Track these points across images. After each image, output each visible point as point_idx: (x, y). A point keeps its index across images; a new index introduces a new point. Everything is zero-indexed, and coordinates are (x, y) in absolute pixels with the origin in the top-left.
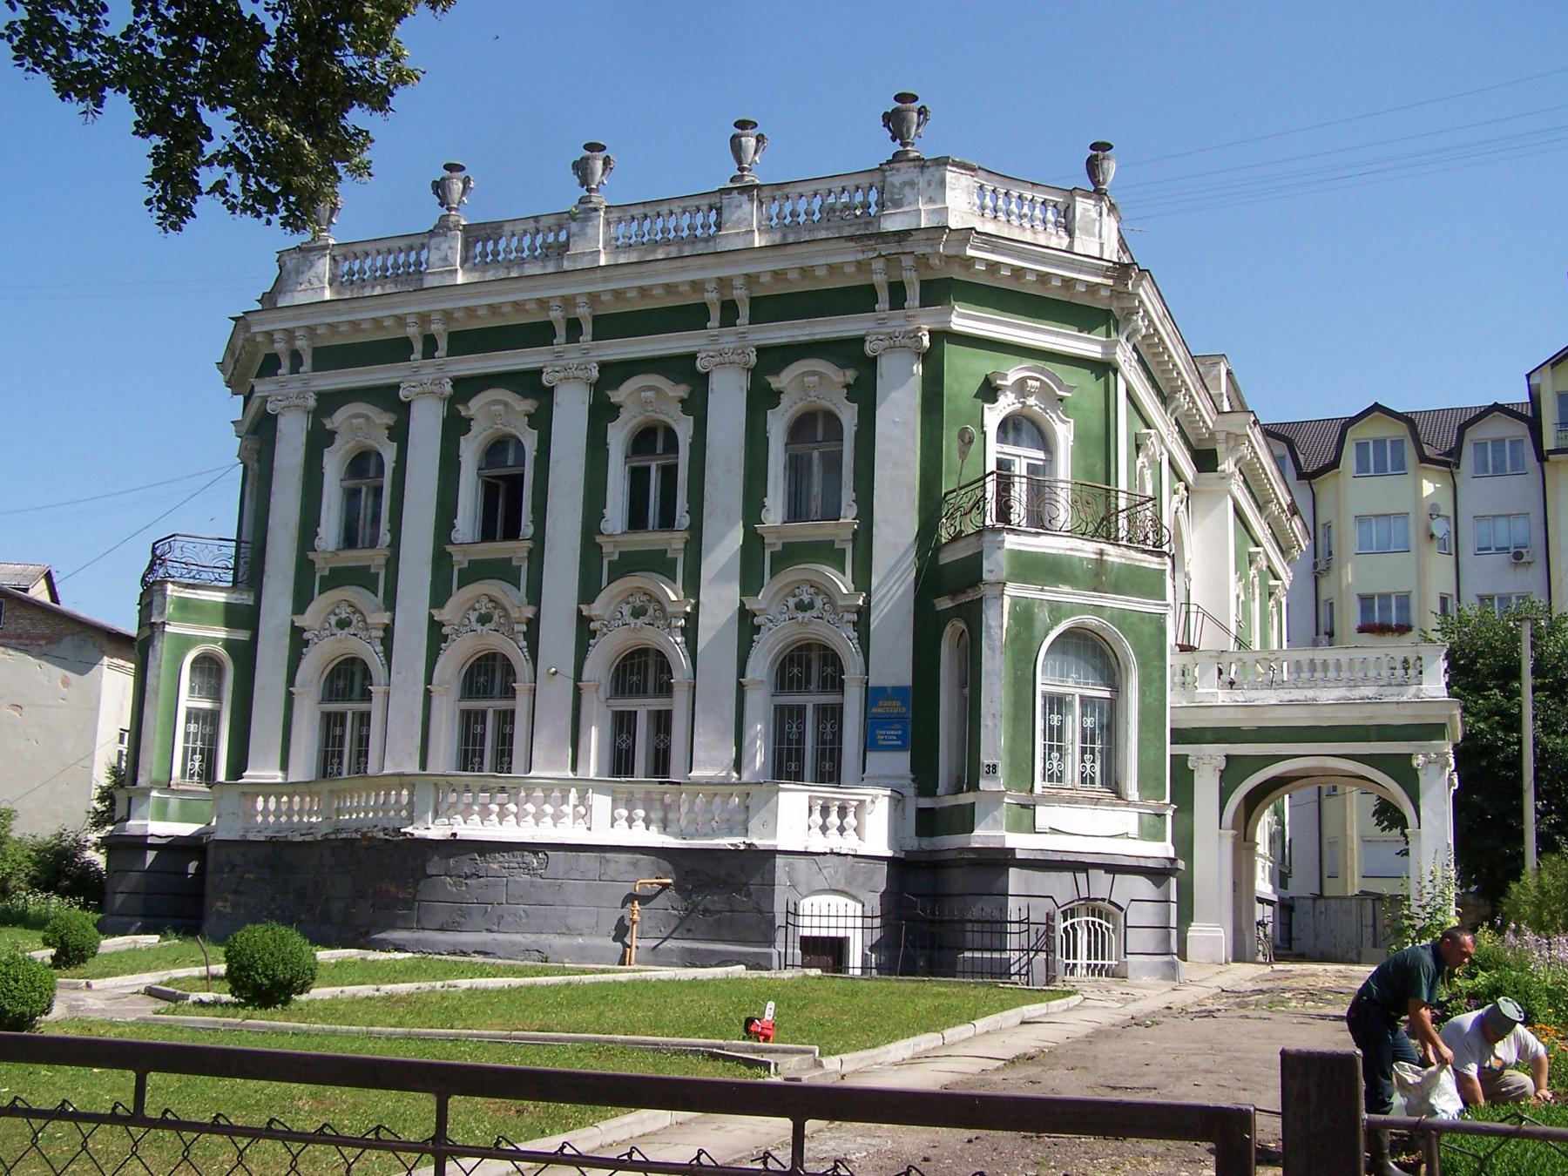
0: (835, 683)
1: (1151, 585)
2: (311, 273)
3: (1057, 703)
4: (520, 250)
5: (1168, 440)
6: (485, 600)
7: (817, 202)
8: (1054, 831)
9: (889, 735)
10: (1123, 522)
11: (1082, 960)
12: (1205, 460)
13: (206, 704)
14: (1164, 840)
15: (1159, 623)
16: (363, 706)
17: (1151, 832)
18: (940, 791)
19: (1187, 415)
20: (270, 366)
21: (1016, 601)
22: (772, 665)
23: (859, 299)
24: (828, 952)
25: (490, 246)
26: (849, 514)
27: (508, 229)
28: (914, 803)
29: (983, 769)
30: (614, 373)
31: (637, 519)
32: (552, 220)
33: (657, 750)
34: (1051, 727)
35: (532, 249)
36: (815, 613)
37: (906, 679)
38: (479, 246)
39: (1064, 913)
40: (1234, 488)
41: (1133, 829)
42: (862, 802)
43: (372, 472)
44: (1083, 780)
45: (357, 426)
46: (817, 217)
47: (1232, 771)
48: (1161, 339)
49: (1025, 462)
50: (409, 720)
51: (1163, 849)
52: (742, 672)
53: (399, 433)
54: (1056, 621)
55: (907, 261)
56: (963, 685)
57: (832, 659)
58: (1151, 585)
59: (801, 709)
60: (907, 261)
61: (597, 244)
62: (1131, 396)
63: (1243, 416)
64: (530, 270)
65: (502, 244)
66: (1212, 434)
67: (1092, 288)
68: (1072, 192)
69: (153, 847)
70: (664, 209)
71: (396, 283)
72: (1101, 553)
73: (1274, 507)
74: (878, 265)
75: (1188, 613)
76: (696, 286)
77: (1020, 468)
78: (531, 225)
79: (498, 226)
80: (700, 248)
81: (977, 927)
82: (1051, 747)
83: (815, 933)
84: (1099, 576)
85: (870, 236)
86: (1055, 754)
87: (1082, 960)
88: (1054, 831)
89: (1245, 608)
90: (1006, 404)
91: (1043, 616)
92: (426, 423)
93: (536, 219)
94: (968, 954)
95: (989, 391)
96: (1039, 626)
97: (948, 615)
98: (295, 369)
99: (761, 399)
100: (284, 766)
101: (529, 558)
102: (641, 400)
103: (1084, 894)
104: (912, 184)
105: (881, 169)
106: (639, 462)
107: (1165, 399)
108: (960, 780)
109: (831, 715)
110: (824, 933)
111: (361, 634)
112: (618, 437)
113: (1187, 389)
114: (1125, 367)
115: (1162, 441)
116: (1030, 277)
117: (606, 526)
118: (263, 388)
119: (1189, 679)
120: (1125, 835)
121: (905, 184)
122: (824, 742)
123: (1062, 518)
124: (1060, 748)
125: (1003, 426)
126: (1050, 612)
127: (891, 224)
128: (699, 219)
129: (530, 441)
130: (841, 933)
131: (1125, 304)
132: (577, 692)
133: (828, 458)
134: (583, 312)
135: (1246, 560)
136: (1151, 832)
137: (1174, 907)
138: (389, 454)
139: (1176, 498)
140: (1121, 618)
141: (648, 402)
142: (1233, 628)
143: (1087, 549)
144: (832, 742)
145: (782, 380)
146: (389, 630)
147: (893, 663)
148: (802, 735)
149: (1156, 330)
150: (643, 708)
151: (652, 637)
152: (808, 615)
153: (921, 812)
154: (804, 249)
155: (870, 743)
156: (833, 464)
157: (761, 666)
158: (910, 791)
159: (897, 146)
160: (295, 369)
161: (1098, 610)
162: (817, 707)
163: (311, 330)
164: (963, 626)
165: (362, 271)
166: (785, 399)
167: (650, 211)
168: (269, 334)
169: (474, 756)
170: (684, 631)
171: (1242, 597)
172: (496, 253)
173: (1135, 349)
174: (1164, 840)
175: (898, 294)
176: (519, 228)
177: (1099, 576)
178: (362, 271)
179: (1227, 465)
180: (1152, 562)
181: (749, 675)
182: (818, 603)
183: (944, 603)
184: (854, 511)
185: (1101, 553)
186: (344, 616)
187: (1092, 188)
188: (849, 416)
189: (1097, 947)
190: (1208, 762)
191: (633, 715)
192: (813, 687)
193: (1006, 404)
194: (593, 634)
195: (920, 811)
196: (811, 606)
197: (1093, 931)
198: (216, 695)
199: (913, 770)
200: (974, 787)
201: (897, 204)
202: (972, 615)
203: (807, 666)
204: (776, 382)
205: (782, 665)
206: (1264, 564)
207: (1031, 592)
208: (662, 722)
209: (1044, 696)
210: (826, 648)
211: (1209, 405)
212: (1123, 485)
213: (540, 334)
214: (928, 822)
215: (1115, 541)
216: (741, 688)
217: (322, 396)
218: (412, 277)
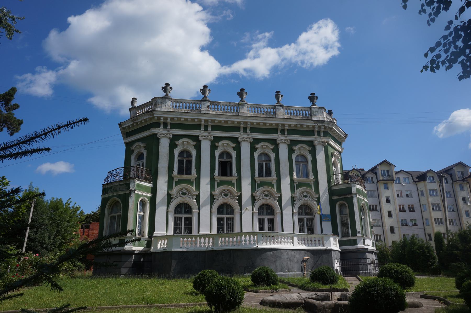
2: (166, 104)
6: (226, 191)
8: (367, 245)
13: (142, 214)
26: (312, 177)
30: (257, 141)
32: (233, 104)
37: (329, 213)
50: (248, 220)
55: (323, 127)
61: (281, 113)
69: (135, 254)
71: (191, 111)
74: (317, 127)
76: (277, 125)
78: (228, 104)
79: (220, 103)
88: (367, 245)
97: (337, 201)
100: (167, 231)
104: (317, 112)
109: (311, 221)
111: (190, 197)
121: (316, 111)
127: (314, 119)
129: (234, 154)
133: (306, 166)
141: (265, 148)
147: (327, 211)
151: (270, 201)
162: (307, 219)
166: (295, 152)
168: (159, 118)
169: (220, 229)
175: (319, 134)
186: (184, 192)
198: (143, 211)
201: (315, 115)
204: (294, 148)
208: (271, 222)
210: (307, 206)
218: (199, 111)
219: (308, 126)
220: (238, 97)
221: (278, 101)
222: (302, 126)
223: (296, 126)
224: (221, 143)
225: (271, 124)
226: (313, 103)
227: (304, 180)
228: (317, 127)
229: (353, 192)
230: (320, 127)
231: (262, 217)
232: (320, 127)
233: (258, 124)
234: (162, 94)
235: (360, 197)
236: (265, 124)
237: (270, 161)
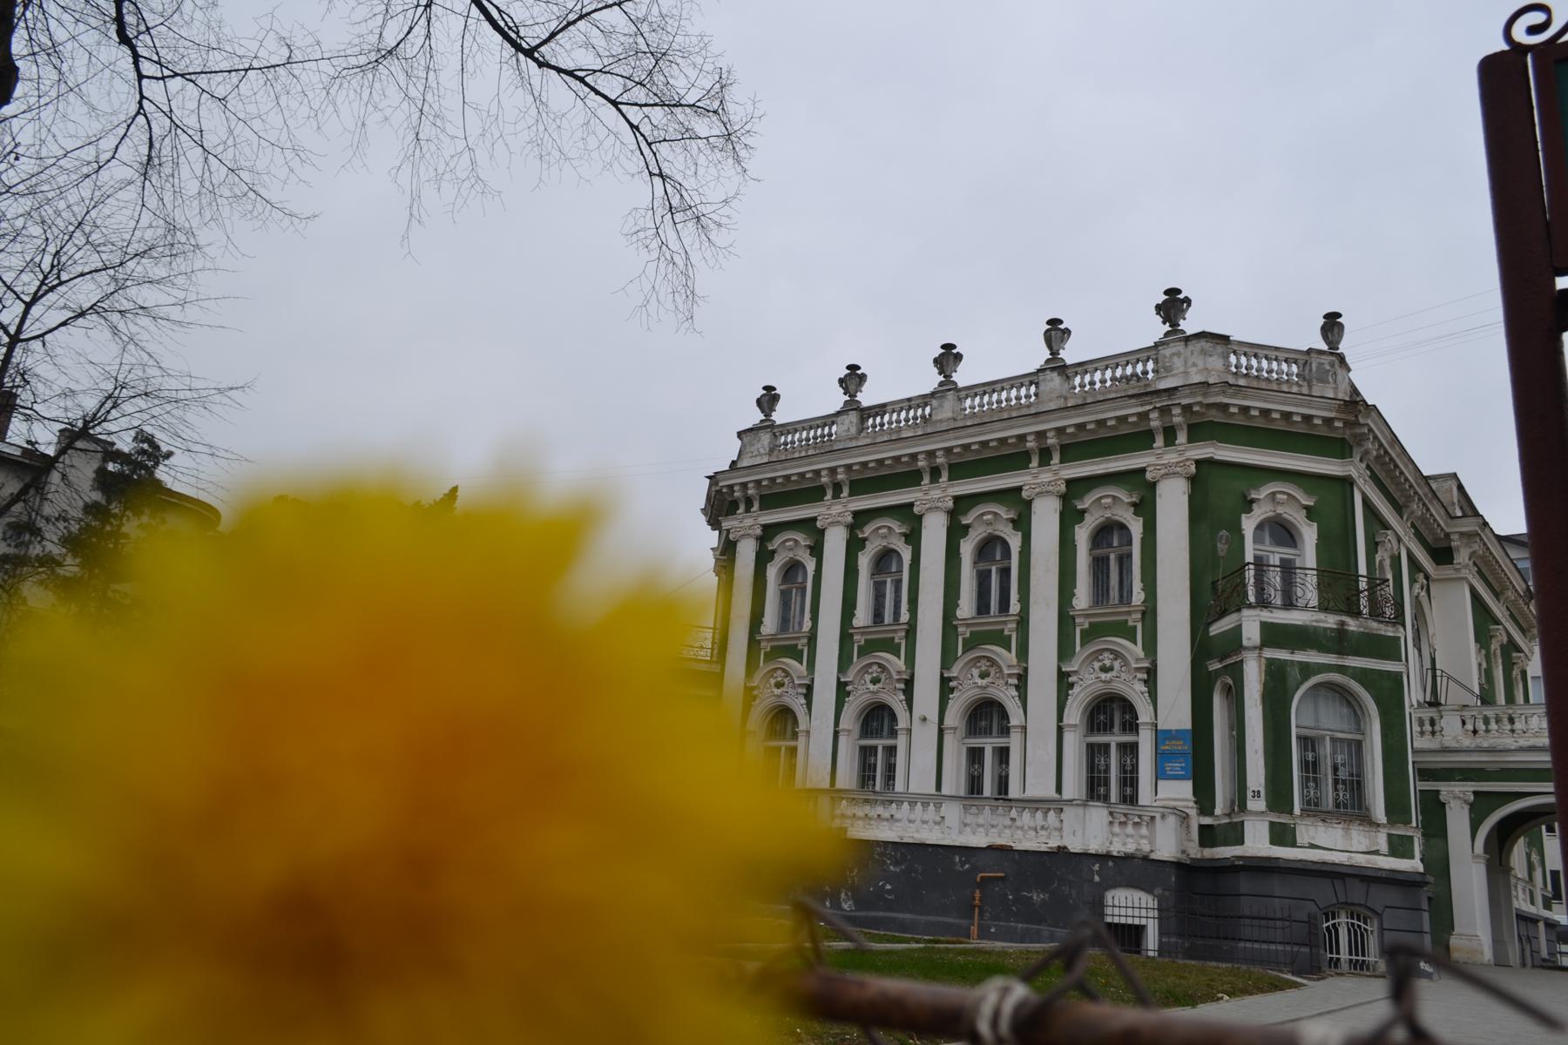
0: (1132, 726)
1: (1389, 649)
3: (1308, 743)
4: (898, 421)
5: (1405, 539)
6: (875, 668)
7: (1109, 374)
8: (1313, 846)
9: (1175, 767)
10: (1363, 602)
11: (1344, 955)
12: (1442, 555)
14: (1412, 857)
15: (1396, 680)
16: (792, 743)
17: (1399, 847)
18: (1218, 811)
19: (1423, 519)
20: (732, 508)
21: (1271, 663)
22: (1083, 713)
23: (1140, 439)
24: (1131, 935)
25: (878, 419)
27: (889, 408)
28: (1196, 820)
29: (1249, 794)
31: (983, 607)
33: (1000, 777)
34: (1307, 763)
35: (907, 420)
36: (1114, 673)
37: (1188, 726)
38: (871, 421)
39: (1326, 915)
40: (1470, 577)
41: (1383, 846)
42: (1153, 818)
43: (800, 579)
44: (1338, 806)
45: (792, 546)
46: (1108, 384)
47: (1481, 806)
48: (1391, 459)
49: (1277, 557)
51: (1414, 865)
52: (1060, 718)
53: (817, 550)
54: (1305, 678)
56: (1231, 729)
57: (1128, 707)
58: (1389, 649)
59: (1107, 746)
60: (1176, 411)
62: (1367, 502)
63: (1473, 520)
64: (904, 435)
65: (886, 418)
66: (1447, 535)
67: (1328, 421)
68: (1310, 351)
70: (998, 387)
72: (1343, 623)
73: (1510, 594)
75: (1434, 677)
76: (1022, 438)
79: (884, 406)
80: (1024, 412)
81: (1247, 921)
83: (1116, 920)
84: (1340, 642)
85: (1146, 394)
86: (1311, 784)
87: (1344, 955)
89: (1488, 675)
90: (1260, 513)
91: (1295, 673)
92: (835, 542)
93: (909, 400)
94: (1242, 944)
95: (1248, 505)
98: (748, 510)
99: (1070, 517)
101: (907, 637)
102: (981, 522)
103: (1342, 900)
104: (1178, 354)
105: (1157, 345)
106: (982, 566)
107: (1399, 509)
108: (1233, 803)
109: (1130, 750)
110: (1123, 920)
112: (967, 548)
113: (1420, 499)
114: (1360, 482)
115: (1399, 540)
117: (960, 613)
118: (726, 525)
119: (1437, 728)
120: (1376, 853)
122: (1125, 772)
123: (1309, 595)
124: (1315, 780)
125: (1260, 527)
126: (1301, 670)
127: (1163, 385)
128: (1023, 391)
130: (1137, 921)
131: (1358, 431)
132: (941, 732)
134: (940, 460)
135: (1483, 638)
136: (1399, 847)
137: (1426, 916)
138: (811, 566)
139: (1417, 586)
140: (1363, 676)
141: (989, 523)
142: (1477, 691)
143: (1330, 621)
144: (1132, 772)
145: (1085, 503)
146: (809, 688)
147: (1175, 710)
148: (1108, 767)
149: (1386, 452)
150: (989, 744)
152: (1109, 675)
153: (1202, 828)
154: (1099, 407)
155: (1160, 774)
156: (1124, 560)
157: (1074, 715)
158: (1193, 812)
159: (1167, 327)
160: (748, 510)
161: (1341, 669)
163: (758, 482)
164: (1230, 681)
165: (793, 442)
167: (988, 389)
168: (731, 487)
170: (1017, 687)
171: (1484, 665)
172: (882, 425)
173: (1368, 467)
174: (1412, 857)
175: (1170, 434)
176: (897, 407)
177: (1340, 642)
178: (793, 442)
179: (1462, 557)
180: (1389, 631)
181: (1066, 721)
182: (1117, 664)
183: (1215, 666)
184: (1142, 596)
187: (1324, 347)
188: (1136, 527)
189: (1358, 945)
190: (1456, 798)
191: (982, 750)
192: (1116, 728)
193: (1260, 513)
194: (952, 690)
195: (1202, 828)
196: (1111, 669)
197: (1351, 929)
199: (1195, 793)
200: (1243, 807)
202: (1237, 671)
203: (1110, 712)
205: (1092, 713)
206: (1505, 639)
208: (1003, 754)
209: (1299, 737)
211: (1442, 511)
212: (1362, 570)
213: (911, 478)
214: (1208, 836)
215: (1357, 614)
216: (1060, 730)
217: (765, 527)
219: (1122, 420)
220: (936, 371)
221: (1054, 353)
222: (1101, 423)
223: (1081, 427)
224: (867, 531)
225: (1003, 441)
226: (1174, 325)
227: (1106, 614)
228: (1153, 415)
229: (1245, 643)
230: (1165, 411)
231: (976, 742)
232: (1165, 411)
233: (966, 447)
234: (756, 417)
235: (1300, 657)
236: (984, 444)
237: (1130, 543)
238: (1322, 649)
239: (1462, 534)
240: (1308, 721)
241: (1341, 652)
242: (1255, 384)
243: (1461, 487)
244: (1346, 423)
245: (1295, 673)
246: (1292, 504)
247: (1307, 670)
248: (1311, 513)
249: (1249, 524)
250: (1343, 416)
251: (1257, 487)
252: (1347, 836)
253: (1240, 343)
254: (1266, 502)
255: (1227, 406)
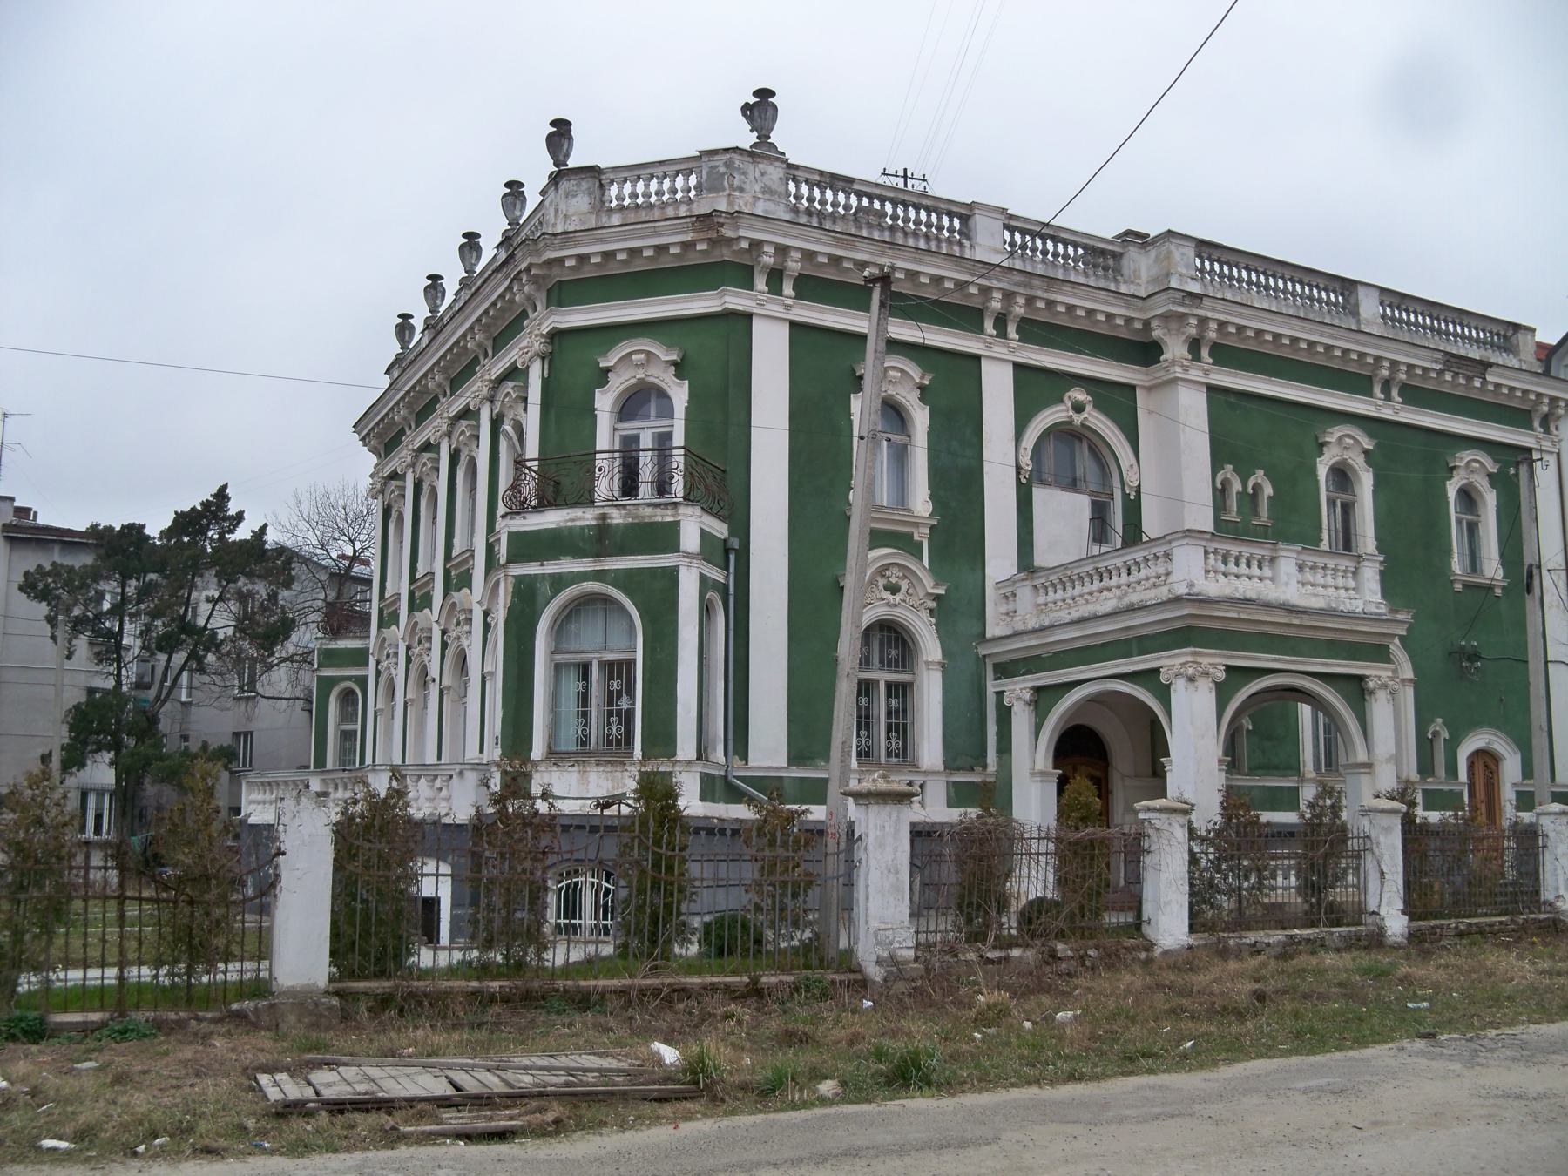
21: (520, 580)
54: (556, 592)
67: (687, 246)
72: (604, 517)
77: (646, 441)
82: (610, 714)
91: (545, 589)
95: (603, 376)
96: (540, 600)
116: (570, 263)
126: (552, 585)
140: (626, 580)
161: (599, 576)
179: (1175, 349)
185: (604, 517)
193: (619, 383)
207: (532, 569)
235: (551, 568)
238: (578, 553)
239: (1166, 318)
240: (617, 639)
241: (598, 555)
242: (632, 217)
243: (1205, 248)
244: (713, 243)
245: (545, 589)
246: (654, 363)
247: (559, 582)
248: (680, 369)
249: (605, 402)
250: (702, 235)
251: (605, 353)
252: (584, 780)
253: (615, 169)
254: (627, 366)
255: (561, 260)
